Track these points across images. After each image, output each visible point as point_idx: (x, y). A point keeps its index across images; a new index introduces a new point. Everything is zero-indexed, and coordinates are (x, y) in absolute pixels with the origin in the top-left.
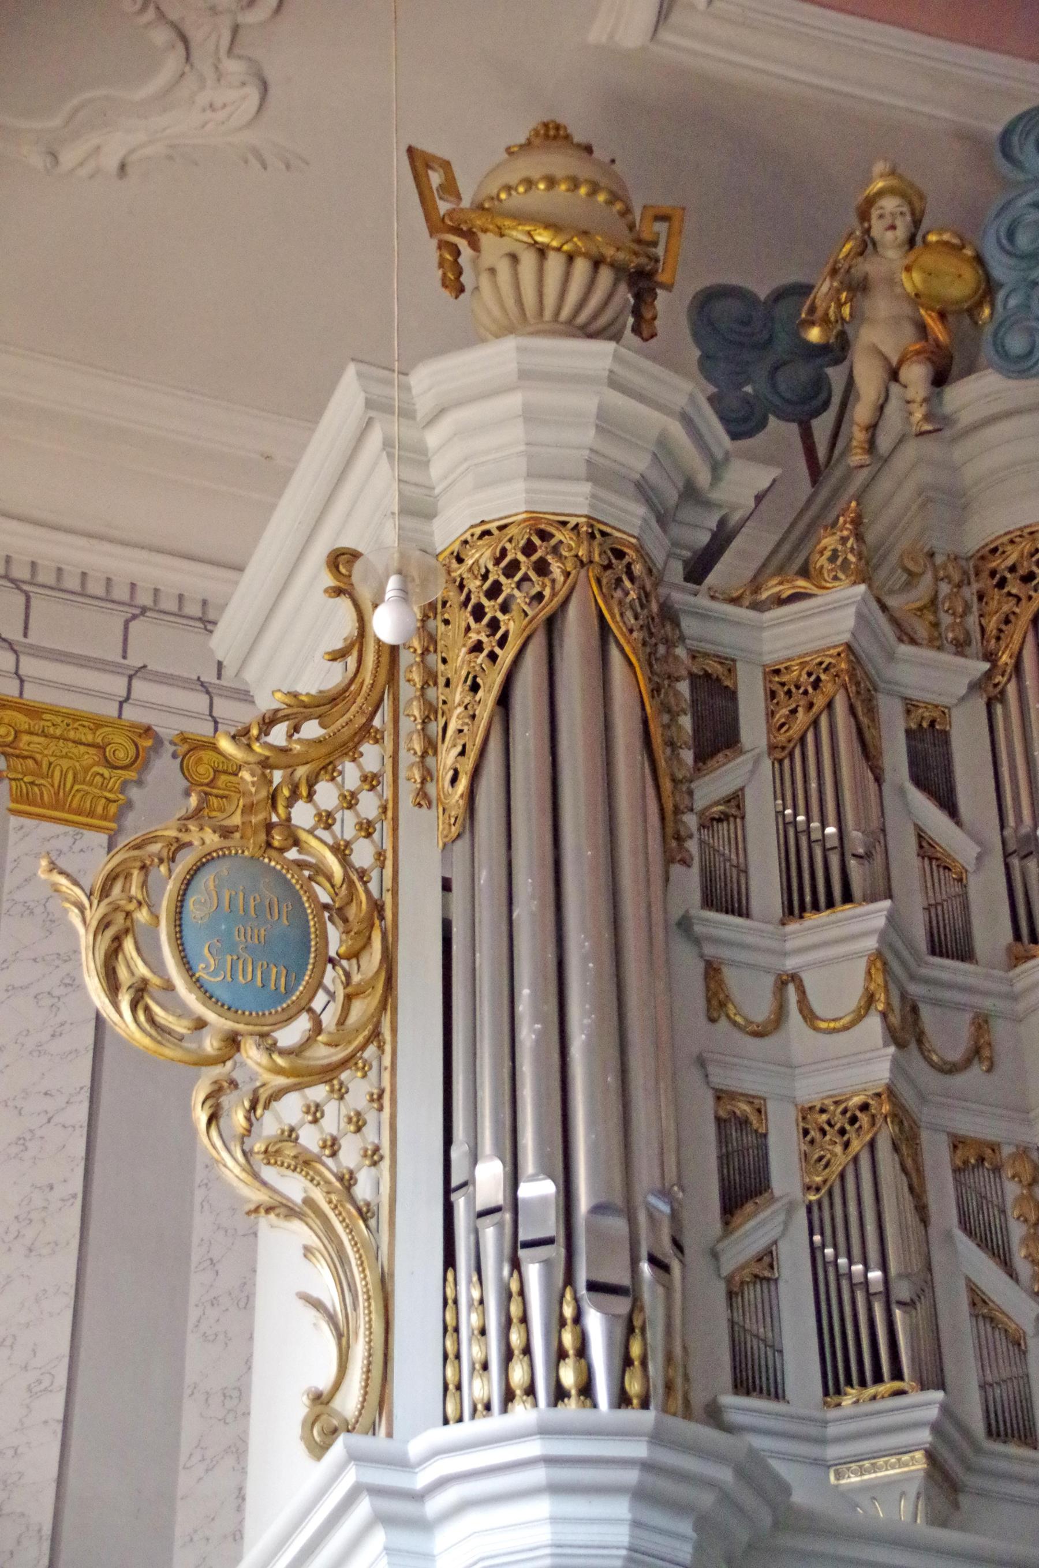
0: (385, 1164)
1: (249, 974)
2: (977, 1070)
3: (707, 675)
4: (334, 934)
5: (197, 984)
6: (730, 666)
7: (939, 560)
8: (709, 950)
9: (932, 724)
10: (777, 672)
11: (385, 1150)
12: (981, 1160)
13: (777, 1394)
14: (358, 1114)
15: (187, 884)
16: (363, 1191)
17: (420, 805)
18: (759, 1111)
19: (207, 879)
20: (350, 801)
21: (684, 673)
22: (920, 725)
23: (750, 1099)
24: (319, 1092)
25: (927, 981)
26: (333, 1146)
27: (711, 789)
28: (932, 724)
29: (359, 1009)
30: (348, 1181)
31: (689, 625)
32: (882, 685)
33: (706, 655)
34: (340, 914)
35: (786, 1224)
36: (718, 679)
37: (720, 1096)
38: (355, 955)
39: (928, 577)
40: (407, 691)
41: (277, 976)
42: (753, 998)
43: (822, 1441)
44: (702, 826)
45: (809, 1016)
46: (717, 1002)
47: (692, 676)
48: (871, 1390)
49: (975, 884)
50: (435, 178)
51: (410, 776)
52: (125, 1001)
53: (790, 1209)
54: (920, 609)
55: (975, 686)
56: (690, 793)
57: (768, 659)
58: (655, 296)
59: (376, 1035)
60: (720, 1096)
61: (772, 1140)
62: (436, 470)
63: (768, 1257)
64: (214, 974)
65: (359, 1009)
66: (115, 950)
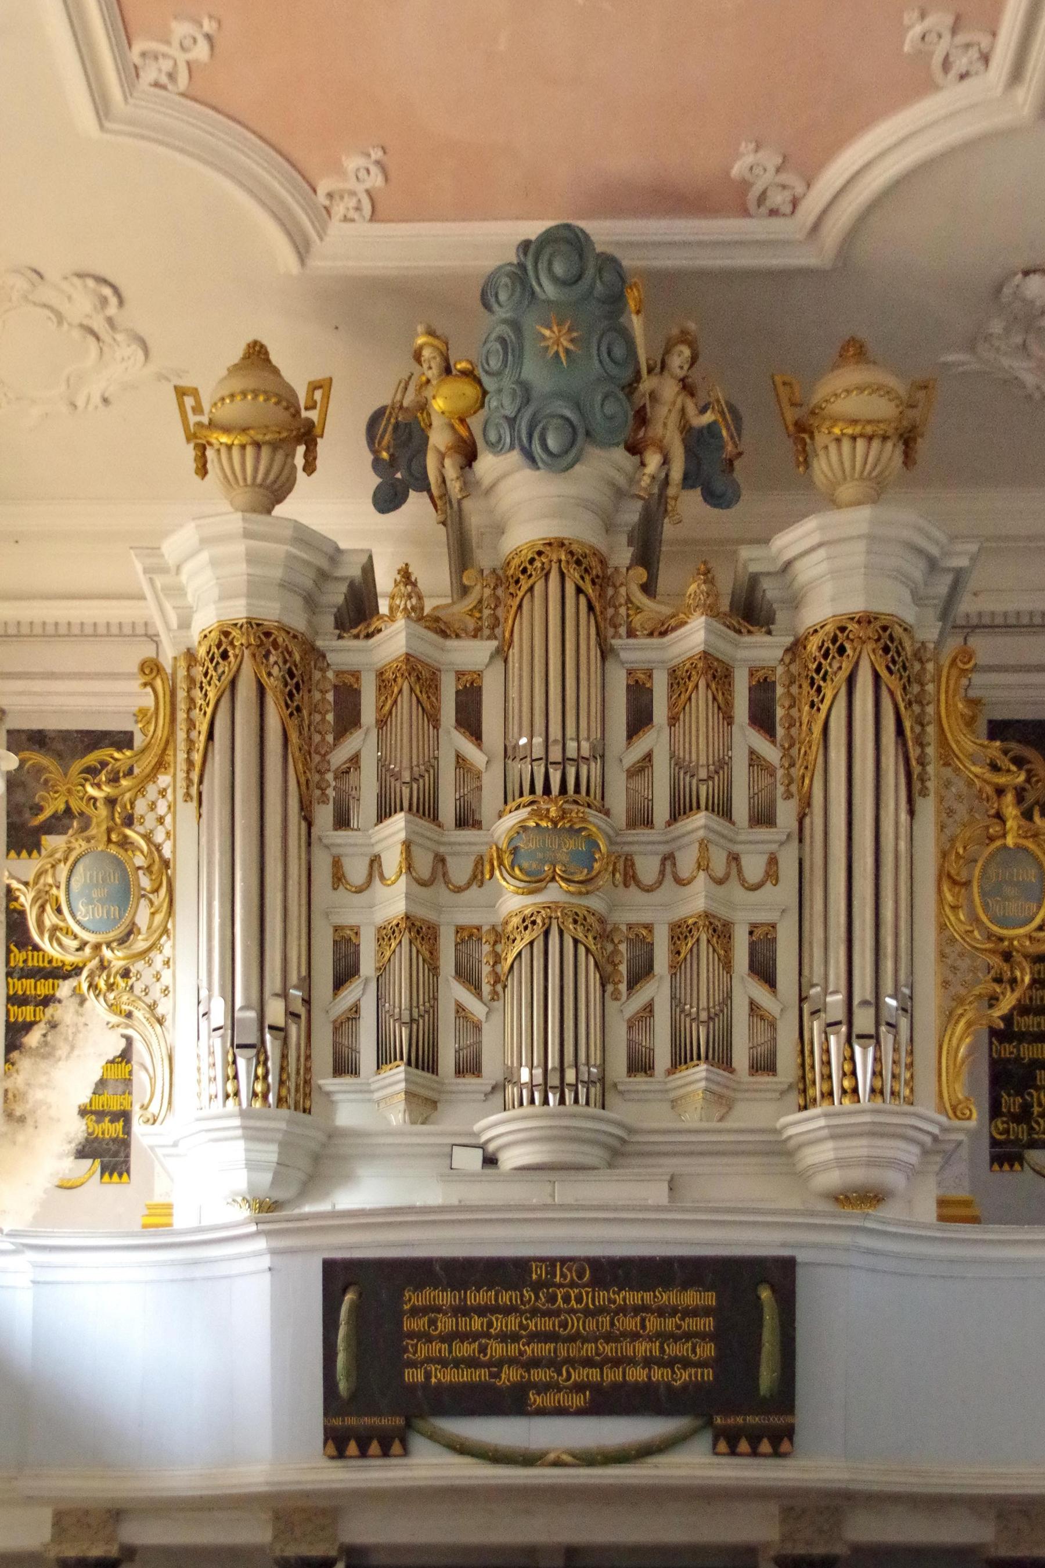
0: (171, 995)
1: (100, 913)
2: (474, 887)
3: (345, 684)
4: (145, 882)
5: (78, 923)
6: (356, 675)
7: (486, 573)
8: (335, 851)
9: (472, 684)
10: (382, 674)
11: (171, 989)
12: (471, 936)
13: (355, 1072)
14: (158, 973)
15: (71, 872)
16: (160, 1010)
17: (186, 801)
18: (356, 933)
19: (80, 868)
20: (153, 806)
21: (329, 687)
22: (465, 686)
23: (351, 928)
24: (139, 966)
25: (450, 844)
26: (146, 990)
27: (339, 757)
28: (472, 684)
29: (159, 918)
30: (152, 1007)
31: (331, 657)
32: (442, 667)
33: (343, 672)
34: (149, 869)
35: (364, 990)
36: (351, 686)
37: (336, 929)
38: (156, 891)
39: (478, 587)
40: (181, 735)
41: (114, 910)
42: (356, 871)
43: (372, 1092)
44: (335, 778)
45: (382, 877)
46: (338, 878)
47: (335, 687)
48: (390, 1066)
49: (486, 779)
50: (189, 402)
51: (181, 783)
52: (46, 936)
53: (367, 980)
54: (471, 610)
55: (492, 657)
56: (329, 762)
57: (379, 665)
58: (316, 444)
59: (166, 931)
60: (336, 929)
61: (362, 948)
62: (190, 598)
63: (356, 1009)
64: (85, 916)
65: (159, 918)
66: (42, 908)
